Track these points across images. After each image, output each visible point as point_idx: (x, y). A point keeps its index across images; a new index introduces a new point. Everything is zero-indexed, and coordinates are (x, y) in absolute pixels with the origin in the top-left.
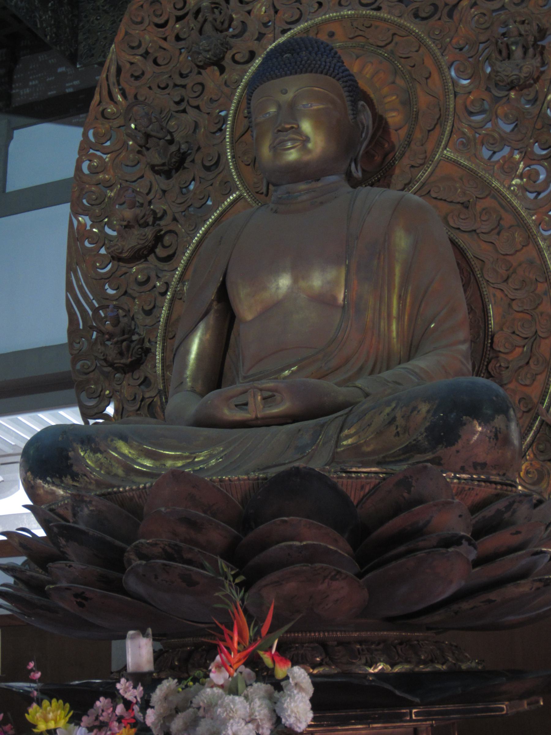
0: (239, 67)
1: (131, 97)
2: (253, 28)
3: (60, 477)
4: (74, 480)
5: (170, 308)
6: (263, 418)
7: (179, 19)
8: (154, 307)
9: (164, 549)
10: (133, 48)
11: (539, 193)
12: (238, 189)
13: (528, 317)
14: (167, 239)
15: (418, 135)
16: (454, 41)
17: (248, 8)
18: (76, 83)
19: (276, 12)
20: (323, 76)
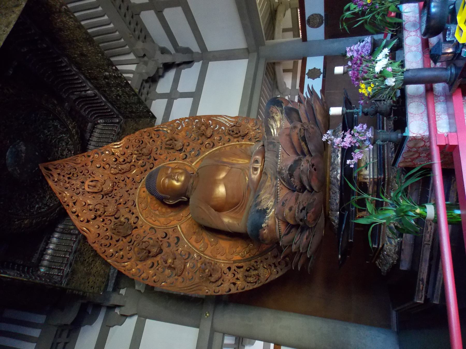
2: (129, 216)
3: (267, 213)
4: (269, 209)
5: (206, 255)
7: (111, 239)
19: (127, 207)
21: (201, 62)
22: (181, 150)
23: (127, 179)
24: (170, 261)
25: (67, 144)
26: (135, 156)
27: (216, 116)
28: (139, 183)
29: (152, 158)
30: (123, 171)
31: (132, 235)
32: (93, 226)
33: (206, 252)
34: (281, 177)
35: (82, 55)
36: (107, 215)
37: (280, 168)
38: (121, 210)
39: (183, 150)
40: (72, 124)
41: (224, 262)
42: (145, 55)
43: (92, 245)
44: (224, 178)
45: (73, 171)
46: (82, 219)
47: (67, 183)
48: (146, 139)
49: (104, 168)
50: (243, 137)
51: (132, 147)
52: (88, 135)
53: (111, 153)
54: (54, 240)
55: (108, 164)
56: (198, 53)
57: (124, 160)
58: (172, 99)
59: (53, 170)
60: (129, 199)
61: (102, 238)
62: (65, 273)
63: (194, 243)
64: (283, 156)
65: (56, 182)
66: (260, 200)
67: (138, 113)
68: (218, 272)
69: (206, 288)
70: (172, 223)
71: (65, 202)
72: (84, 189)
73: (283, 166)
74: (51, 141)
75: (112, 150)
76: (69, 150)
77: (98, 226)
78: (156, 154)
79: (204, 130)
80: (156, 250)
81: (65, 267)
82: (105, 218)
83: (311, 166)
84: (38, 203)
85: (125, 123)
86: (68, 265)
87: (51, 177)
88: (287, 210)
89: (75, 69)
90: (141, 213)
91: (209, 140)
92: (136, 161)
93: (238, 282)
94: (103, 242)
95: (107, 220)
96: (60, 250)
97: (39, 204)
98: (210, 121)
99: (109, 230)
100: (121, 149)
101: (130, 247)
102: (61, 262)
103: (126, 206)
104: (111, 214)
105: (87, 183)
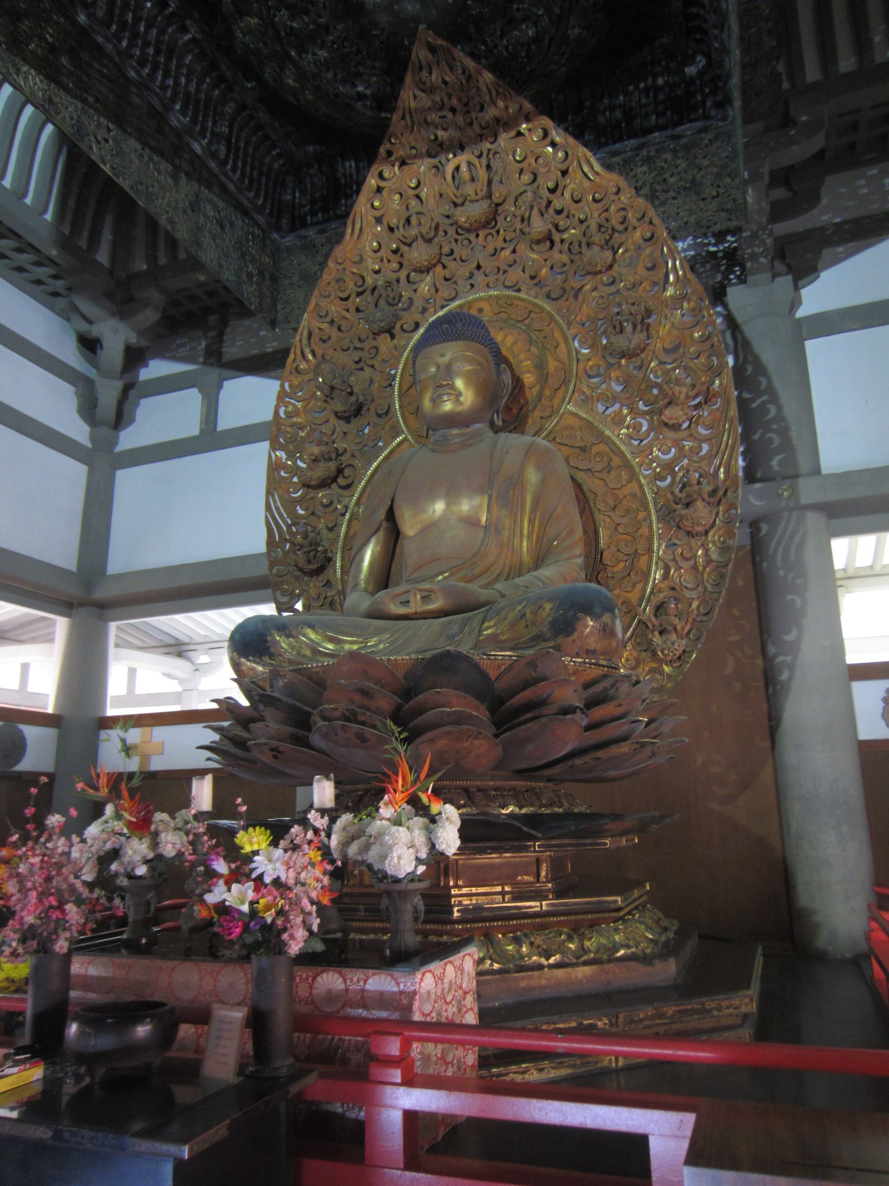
0: (406, 335)
1: (319, 356)
3: (260, 657)
4: (271, 659)
5: (349, 526)
6: (421, 613)
7: (359, 294)
8: (335, 525)
9: (343, 714)
10: (321, 317)
11: (642, 441)
12: (403, 433)
13: (629, 537)
14: (347, 472)
15: (547, 392)
16: (578, 318)
17: (414, 287)
18: (274, 344)
19: (437, 291)
20: (473, 343)
23: (511, 248)
32: (376, 236)
33: (355, 522)
46: (376, 204)
53: (563, 167)
60: (460, 282)
61: (353, 273)
75: (573, 162)
77: (376, 249)
92: (566, 246)
95: (400, 259)
97: (366, 88)
99: (376, 276)
100: (587, 184)
105: (463, 159)
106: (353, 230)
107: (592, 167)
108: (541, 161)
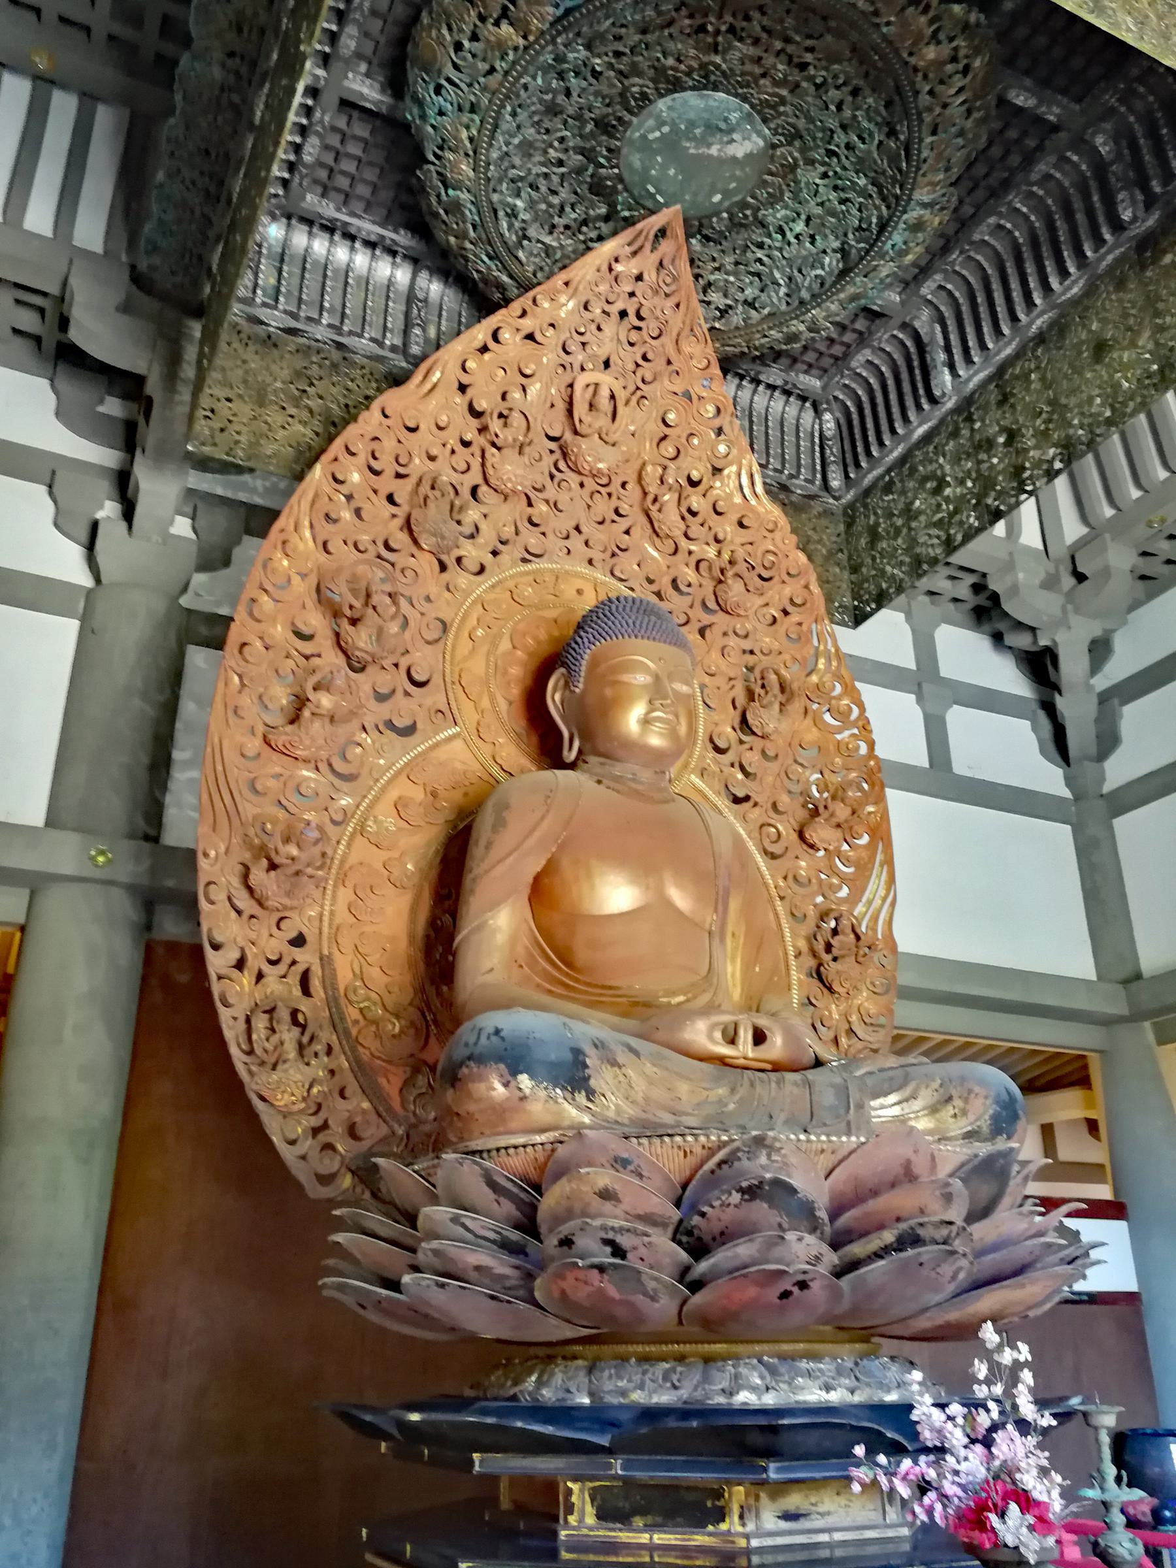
5: (349, 845)
7: (399, 476)
21: (1066, 793)
22: (744, 723)
23: (624, 527)
24: (325, 701)
25: (750, 304)
26: (711, 552)
27: (889, 862)
28: (612, 574)
29: (707, 619)
30: (654, 509)
31: (415, 551)
32: (447, 406)
34: (738, 1149)
35: (1100, 349)
36: (487, 455)
37: (778, 1145)
38: (506, 508)
39: (744, 738)
40: (826, 318)
41: (326, 919)
42: (1080, 578)
43: (376, 406)
44: (669, 904)
45: (651, 327)
46: (470, 365)
47: (607, 308)
48: (779, 593)
49: (665, 438)
50: (818, 974)
51: (744, 540)
52: (774, 374)
54: (384, 268)
55: (679, 451)
56: (1102, 779)
57: (694, 514)
58: (919, 685)
59: (654, 258)
60: (550, 535)
62: (263, 314)
63: (393, 794)
64: (823, 1151)
65: (611, 269)
66: (620, 1060)
67: (874, 558)
68: (288, 894)
69: (222, 848)
70: (467, 706)
71: (534, 301)
72: (583, 369)
73: (784, 1156)
74: (760, 246)
75: (731, 464)
76: (724, 312)
78: (725, 634)
79: (832, 815)
80: (362, 645)
81: (285, 312)
82: (475, 449)
83: (801, 1277)
84: (532, 204)
85: (827, 513)
86: (293, 324)
87: (628, 250)
88: (604, 1178)
89: (1039, 322)
90: (500, 582)
91: (794, 836)
92: (693, 560)
93: (246, 979)
94: (388, 446)
96: (349, 289)
98: (865, 840)
100: (738, 499)
101: (371, 548)
102: (304, 297)
103: (524, 526)
104: (490, 471)
105: (606, 380)
106: (426, 376)
107: (753, 484)
108: (695, 441)
